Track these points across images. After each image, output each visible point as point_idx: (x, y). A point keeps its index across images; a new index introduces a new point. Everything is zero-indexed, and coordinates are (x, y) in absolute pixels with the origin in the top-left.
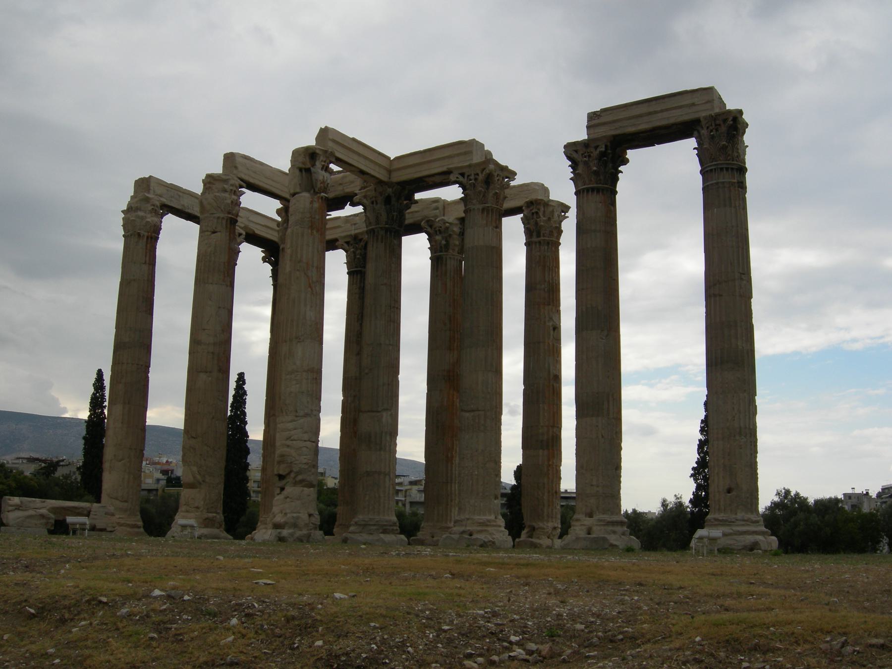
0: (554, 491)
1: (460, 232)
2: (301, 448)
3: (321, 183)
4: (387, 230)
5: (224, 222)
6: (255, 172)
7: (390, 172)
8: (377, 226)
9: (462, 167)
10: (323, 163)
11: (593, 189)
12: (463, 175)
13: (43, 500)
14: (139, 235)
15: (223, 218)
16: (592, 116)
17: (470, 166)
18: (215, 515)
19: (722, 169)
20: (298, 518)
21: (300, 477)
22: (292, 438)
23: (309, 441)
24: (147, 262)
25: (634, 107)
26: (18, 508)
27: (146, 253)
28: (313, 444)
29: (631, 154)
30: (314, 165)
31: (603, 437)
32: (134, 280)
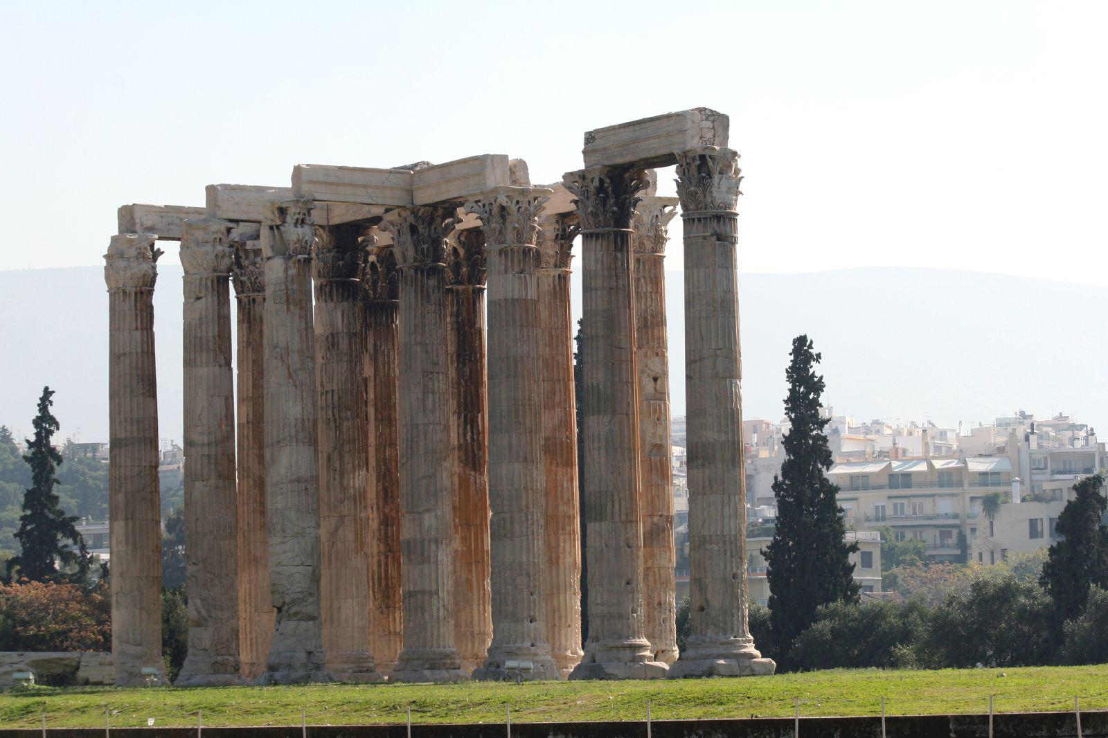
0: (656, 602)
1: (557, 235)
2: (292, 574)
3: (295, 244)
4: (416, 269)
5: (209, 284)
8: (405, 265)
9: (476, 195)
10: (296, 217)
13: (21, 653)
14: (124, 292)
15: (207, 278)
16: (590, 137)
18: (226, 657)
19: (693, 219)
21: (293, 610)
22: (282, 564)
23: (302, 564)
24: (139, 328)
25: (622, 130)
27: (136, 315)
28: (310, 568)
30: (284, 222)
31: (606, 546)
32: (125, 354)
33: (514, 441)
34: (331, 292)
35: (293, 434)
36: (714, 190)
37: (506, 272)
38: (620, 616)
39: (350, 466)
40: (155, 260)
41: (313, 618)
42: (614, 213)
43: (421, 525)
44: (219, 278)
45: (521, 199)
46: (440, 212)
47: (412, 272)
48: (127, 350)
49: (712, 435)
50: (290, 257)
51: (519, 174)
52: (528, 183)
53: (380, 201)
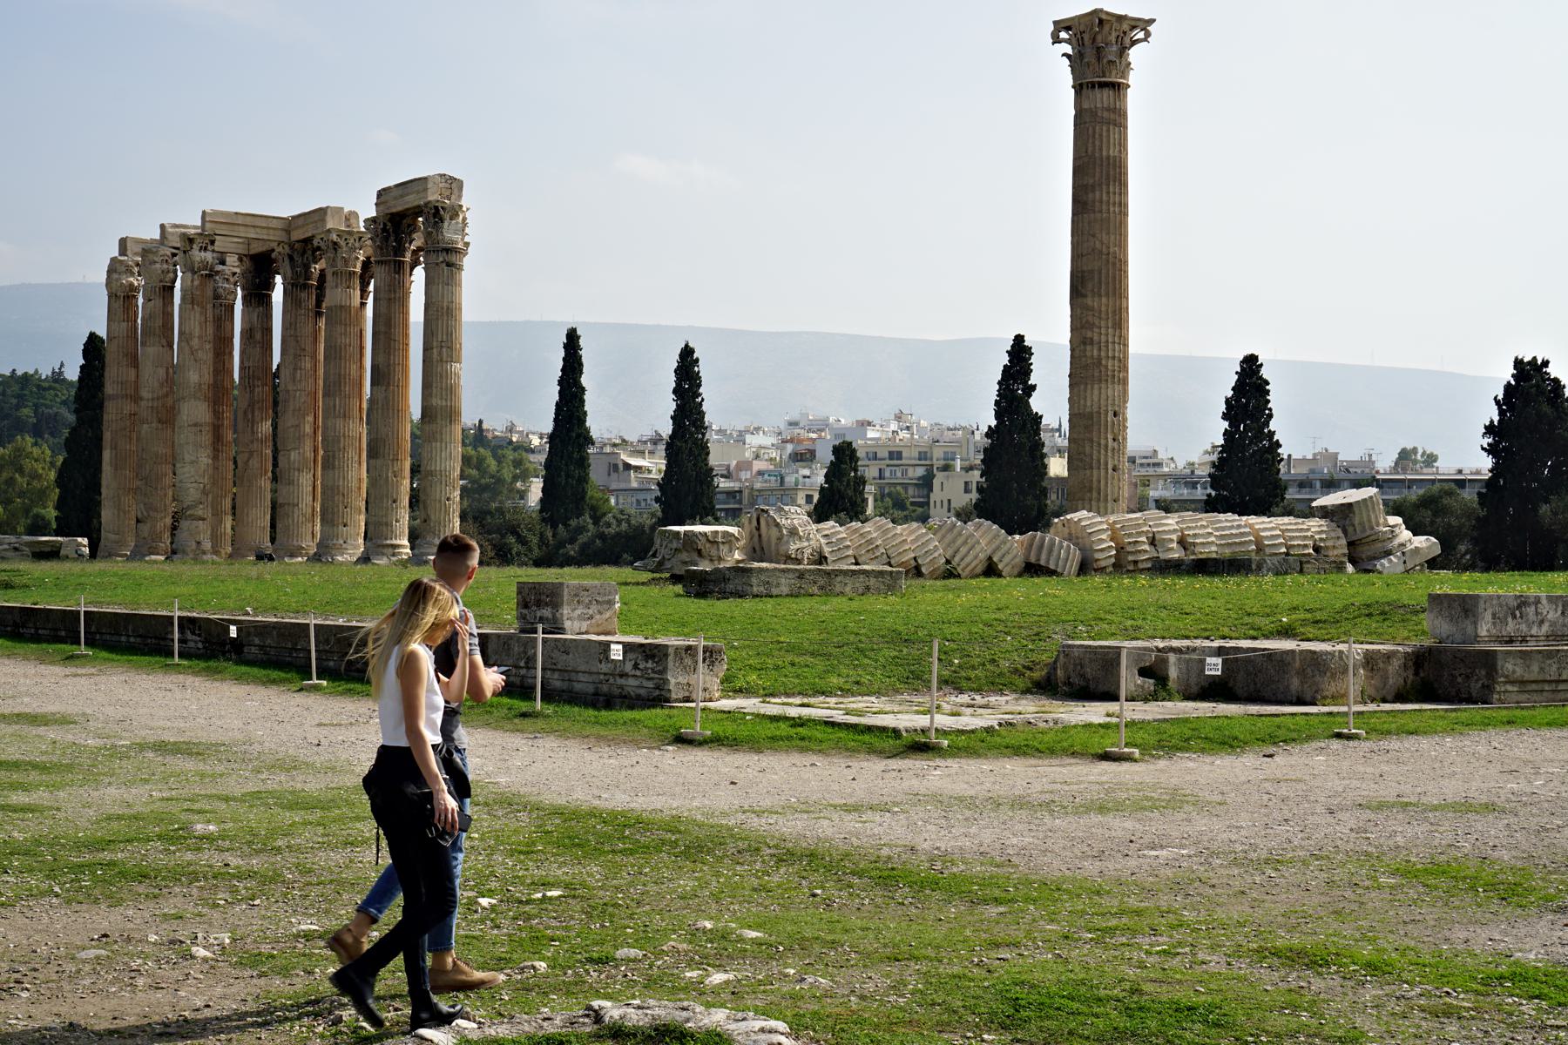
4: (293, 285)
36: (444, 231)
37: (337, 287)
38: (387, 524)
41: (204, 519)
42: (394, 247)
43: (289, 458)
44: (164, 287)
45: (348, 237)
47: (290, 287)
48: (116, 335)
49: (436, 401)
50: (196, 273)
51: (353, 221)
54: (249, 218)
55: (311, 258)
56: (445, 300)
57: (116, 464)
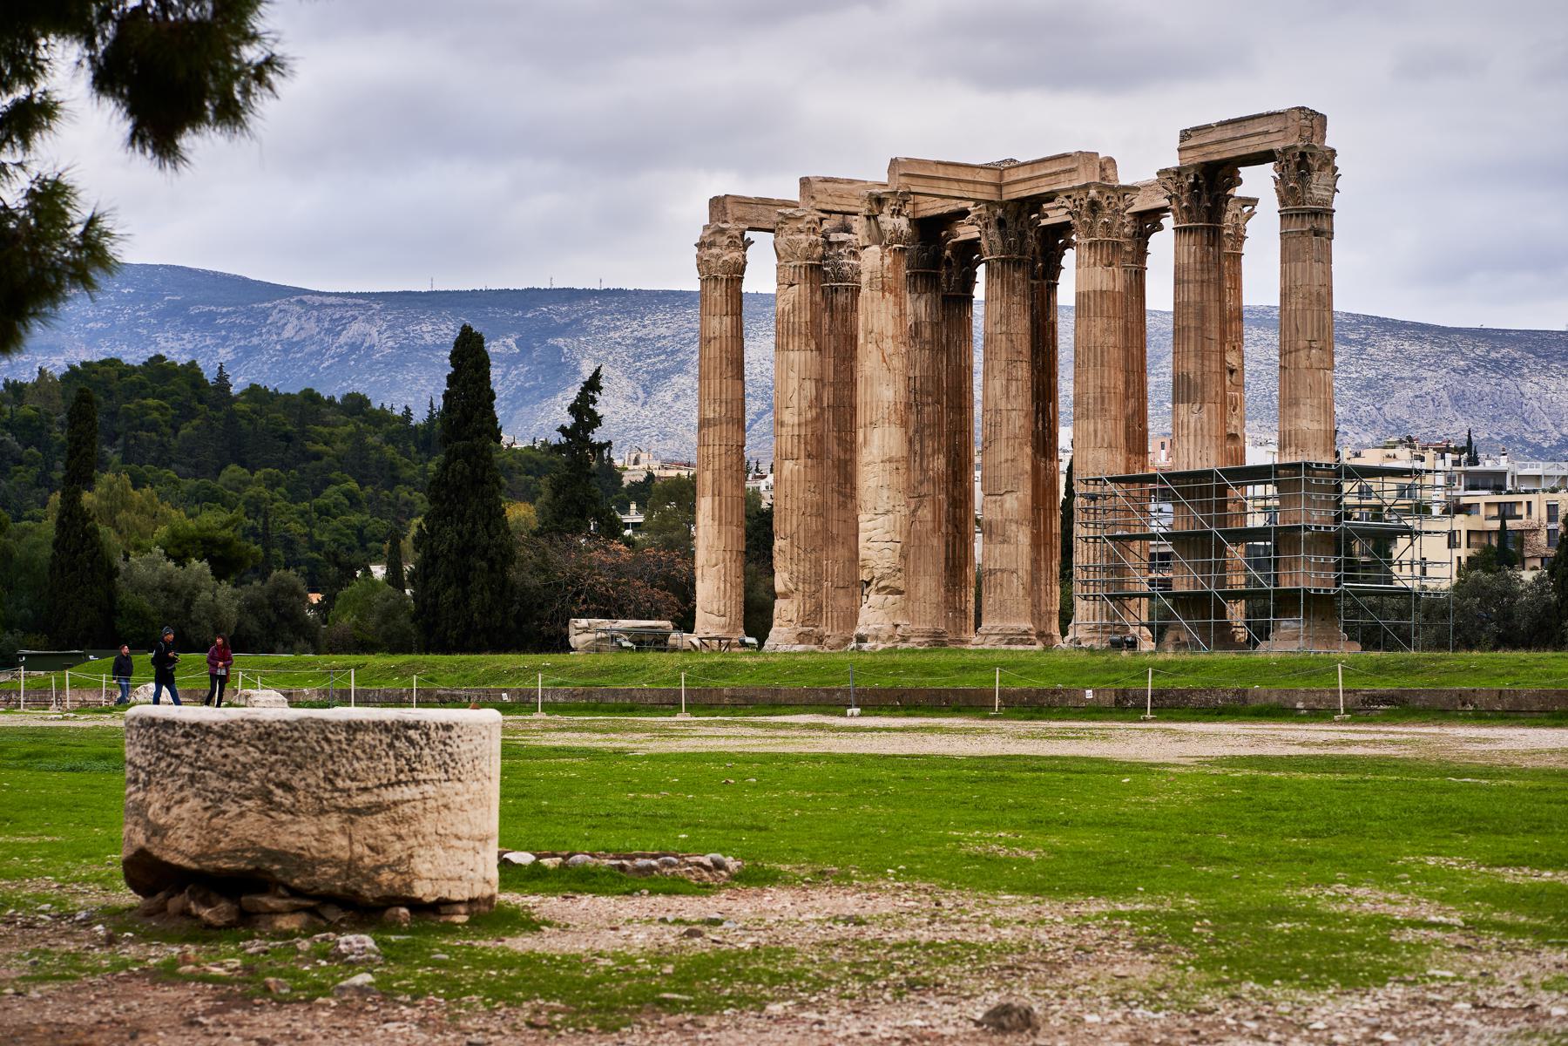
5: (803, 271)
6: (841, 197)
7: (999, 187)
11: (1185, 229)
12: (1068, 197)
14: (716, 278)
16: (1185, 135)
17: (1073, 189)
20: (880, 630)
21: (882, 584)
26: (586, 630)
29: (1245, 172)
30: (881, 212)
33: (1099, 426)
34: (915, 283)
35: (886, 416)
37: (1095, 264)
39: (930, 451)
40: (745, 250)
41: (901, 593)
43: (1001, 506)
46: (1027, 206)
50: (886, 246)
51: (1109, 172)
52: (1117, 180)
53: (971, 196)
54: (951, 169)
55: (1026, 224)
56: (1316, 283)
57: (720, 517)
